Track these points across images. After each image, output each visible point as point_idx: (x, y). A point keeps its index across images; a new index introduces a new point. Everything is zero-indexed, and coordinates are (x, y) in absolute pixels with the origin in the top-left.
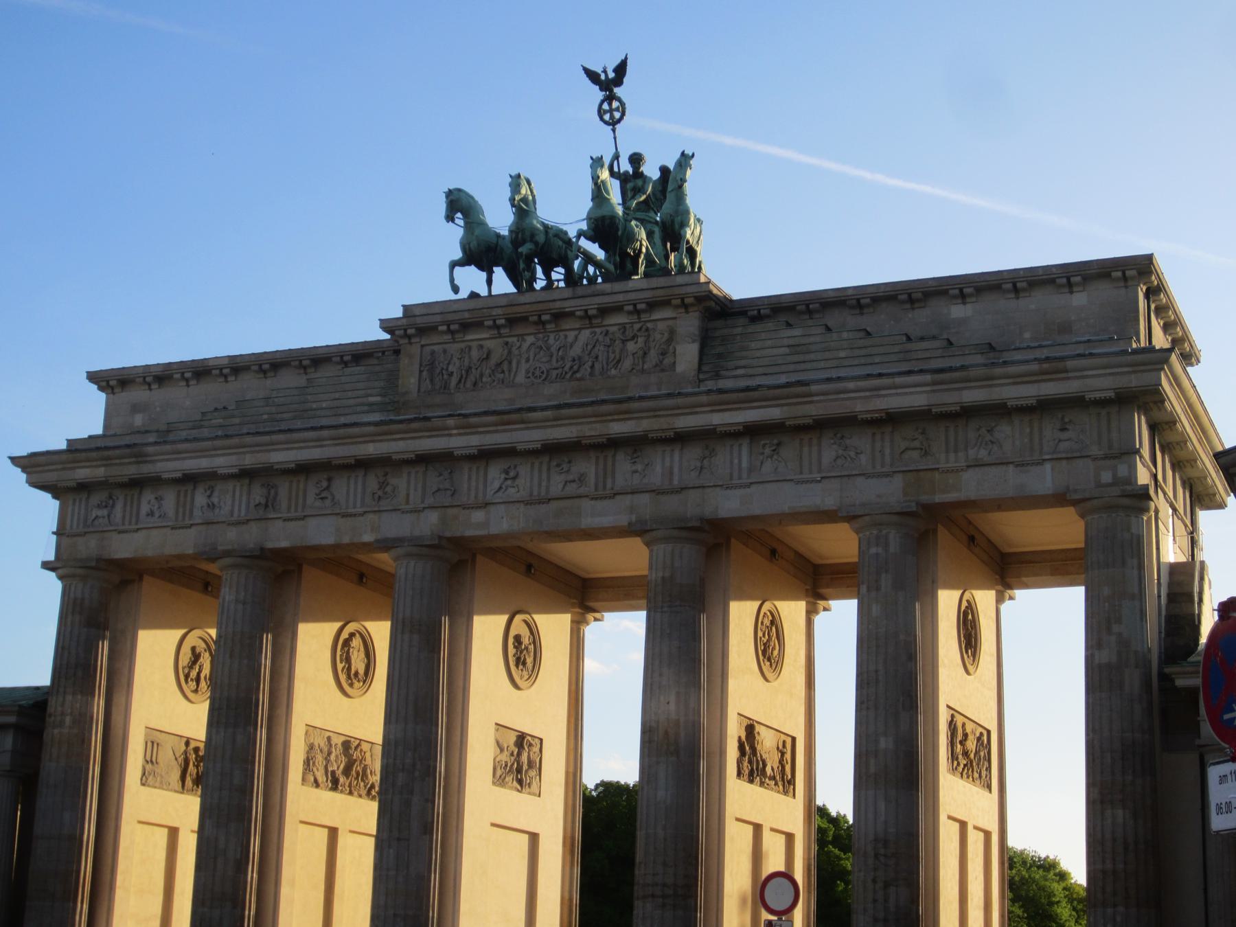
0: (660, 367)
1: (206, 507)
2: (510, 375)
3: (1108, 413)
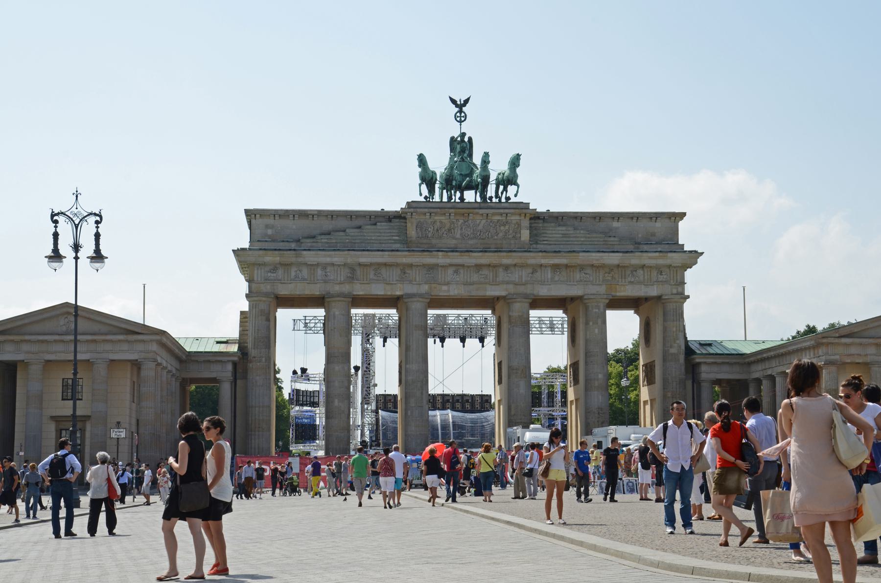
3: (677, 270)
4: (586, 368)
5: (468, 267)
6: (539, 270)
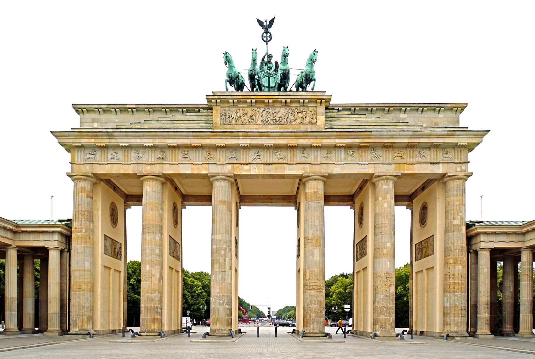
1: (137, 157)
3: (461, 151)
4: (374, 239)
5: (268, 148)
6: (333, 151)
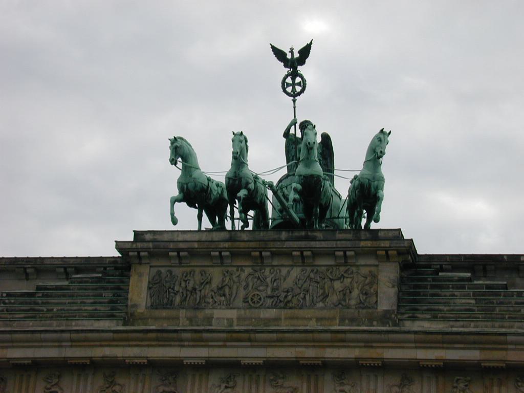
0: (361, 305)
2: (230, 300)
